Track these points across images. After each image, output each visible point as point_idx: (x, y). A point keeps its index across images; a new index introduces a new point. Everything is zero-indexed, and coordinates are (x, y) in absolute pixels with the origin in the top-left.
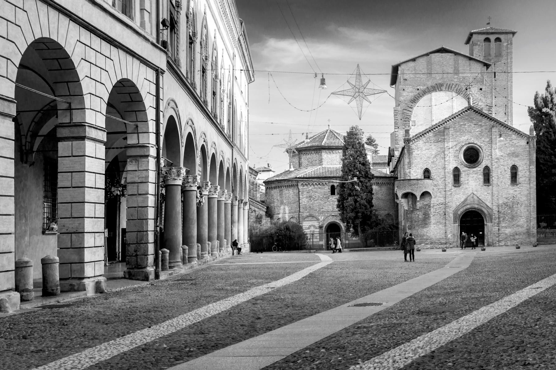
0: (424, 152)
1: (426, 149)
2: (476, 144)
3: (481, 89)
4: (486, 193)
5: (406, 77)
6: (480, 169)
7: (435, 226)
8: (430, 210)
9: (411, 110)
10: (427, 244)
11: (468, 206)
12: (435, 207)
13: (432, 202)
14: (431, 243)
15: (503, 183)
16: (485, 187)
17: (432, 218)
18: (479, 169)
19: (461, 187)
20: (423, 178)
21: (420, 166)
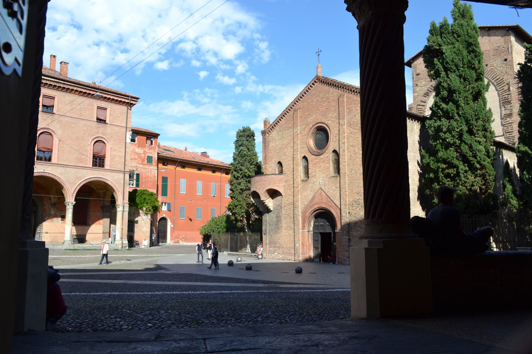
0: (278, 143)
1: (279, 140)
2: (323, 123)
3: (506, 60)
4: (334, 188)
5: (418, 72)
6: (328, 155)
7: (286, 231)
8: (282, 211)
9: (423, 104)
10: (279, 253)
11: (316, 207)
12: (286, 208)
13: (283, 202)
14: (283, 253)
15: (353, 171)
16: (333, 179)
17: (283, 222)
18: (326, 156)
19: (309, 181)
20: (277, 172)
21: (274, 160)
